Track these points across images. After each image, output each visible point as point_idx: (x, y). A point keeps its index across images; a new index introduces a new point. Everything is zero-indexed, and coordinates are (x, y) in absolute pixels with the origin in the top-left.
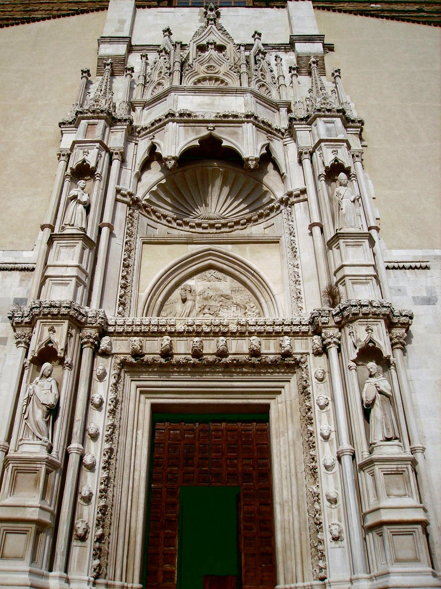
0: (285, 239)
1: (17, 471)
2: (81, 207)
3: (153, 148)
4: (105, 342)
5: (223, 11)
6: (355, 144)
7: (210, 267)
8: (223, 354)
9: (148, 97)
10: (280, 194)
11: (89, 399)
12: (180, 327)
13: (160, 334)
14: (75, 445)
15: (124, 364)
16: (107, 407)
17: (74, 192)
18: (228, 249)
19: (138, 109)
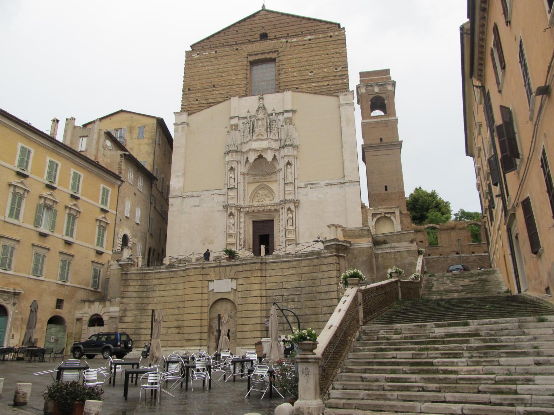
0: (278, 181)
1: (229, 236)
2: (233, 180)
3: (247, 158)
4: (242, 210)
5: (265, 96)
6: (295, 153)
7: (263, 187)
8: (263, 210)
9: (245, 141)
10: (278, 168)
11: (240, 221)
12: (255, 206)
13: (252, 207)
14: (238, 230)
15: (245, 213)
16: (243, 222)
17: (231, 175)
18: (266, 183)
19: (243, 144)
